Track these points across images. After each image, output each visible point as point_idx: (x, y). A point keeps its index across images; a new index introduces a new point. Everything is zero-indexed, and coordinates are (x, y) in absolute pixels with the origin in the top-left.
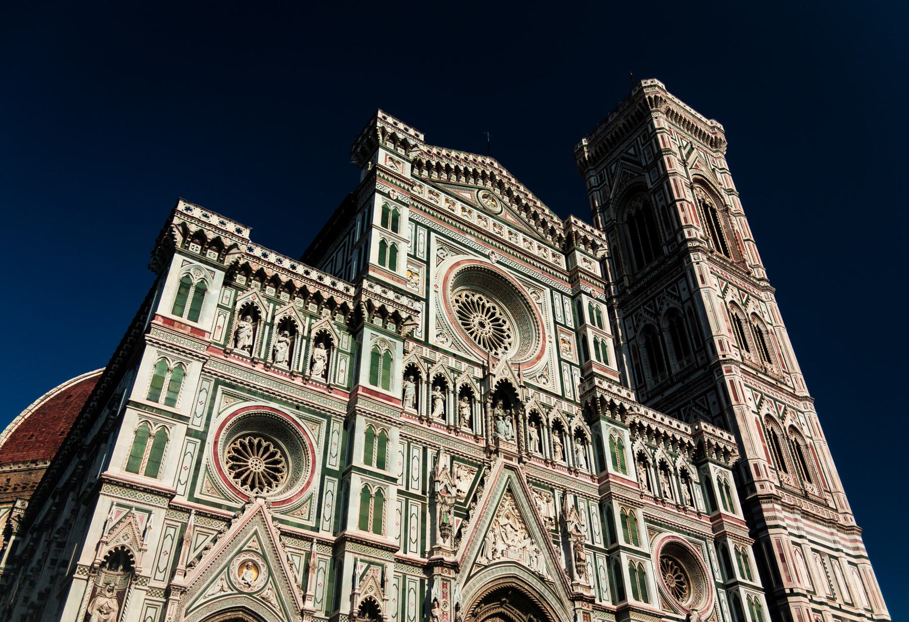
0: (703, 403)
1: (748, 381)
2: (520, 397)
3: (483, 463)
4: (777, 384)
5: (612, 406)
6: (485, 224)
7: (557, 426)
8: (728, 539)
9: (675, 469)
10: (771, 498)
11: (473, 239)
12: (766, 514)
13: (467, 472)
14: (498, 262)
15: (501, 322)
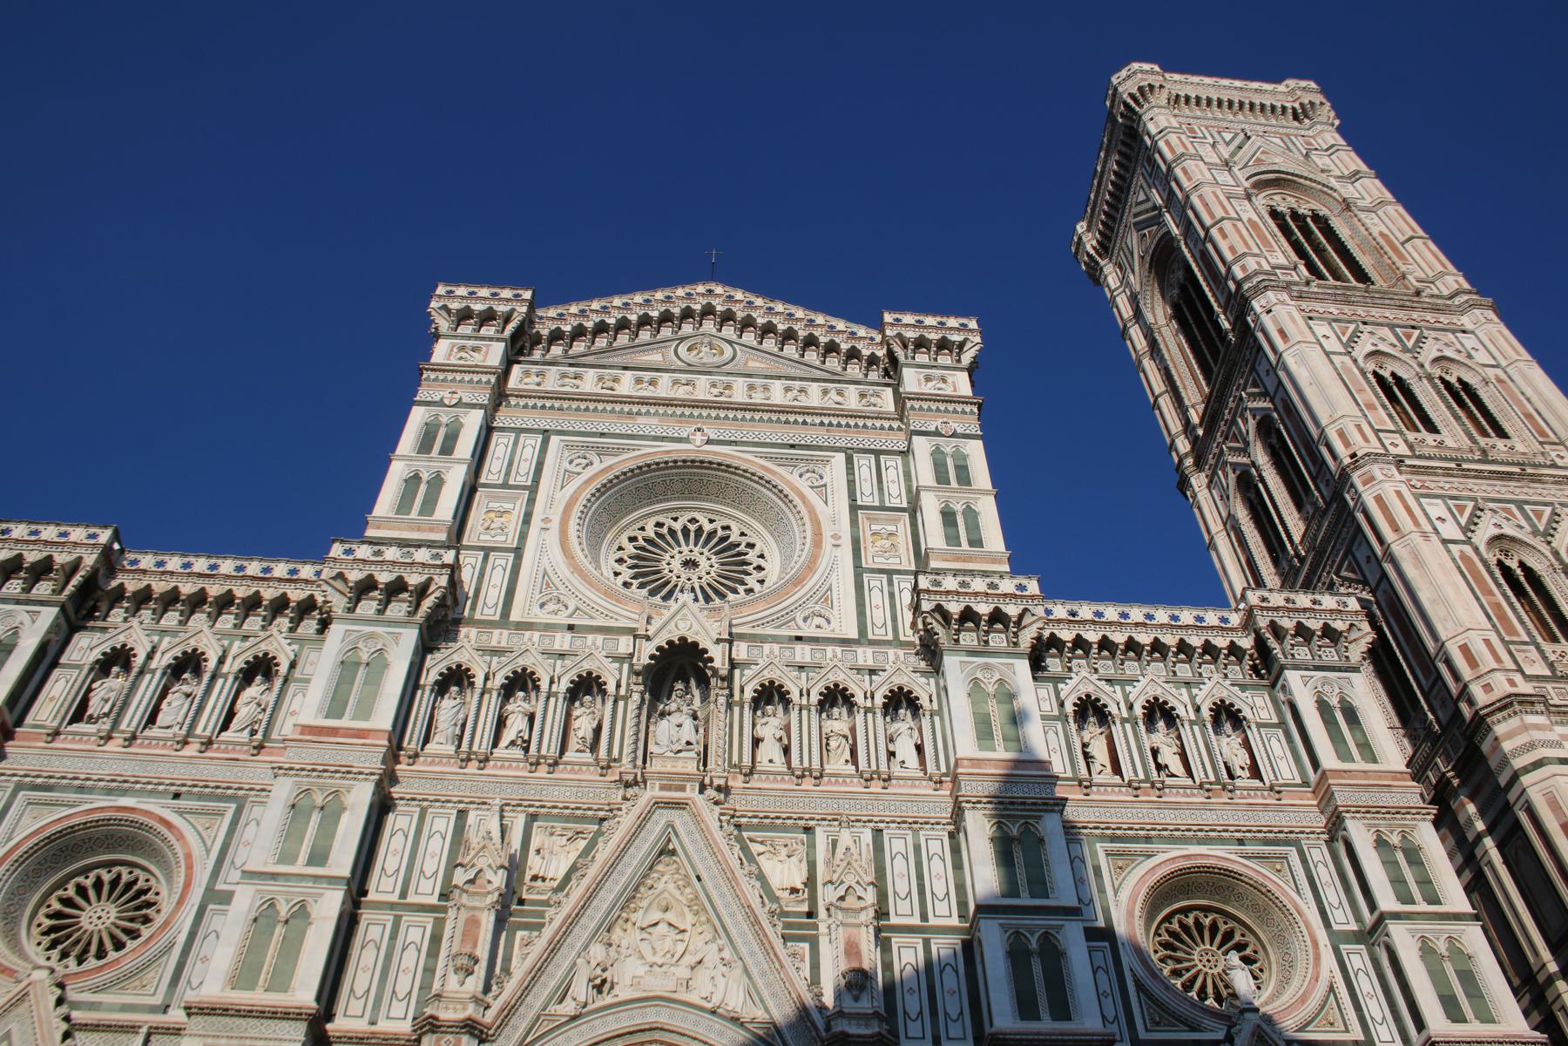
0: (1353, 571)
1: (1432, 485)
2: (717, 664)
3: (611, 810)
4: (1524, 473)
5: (968, 615)
6: (689, 388)
7: (835, 697)
8: (1349, 823)
9: (1198, 710)
10: (1511, 704)
11: (655, 421)
12: (1507, 746)
13: (565, 838)
14: (709, 442)
15: (742, 548)
